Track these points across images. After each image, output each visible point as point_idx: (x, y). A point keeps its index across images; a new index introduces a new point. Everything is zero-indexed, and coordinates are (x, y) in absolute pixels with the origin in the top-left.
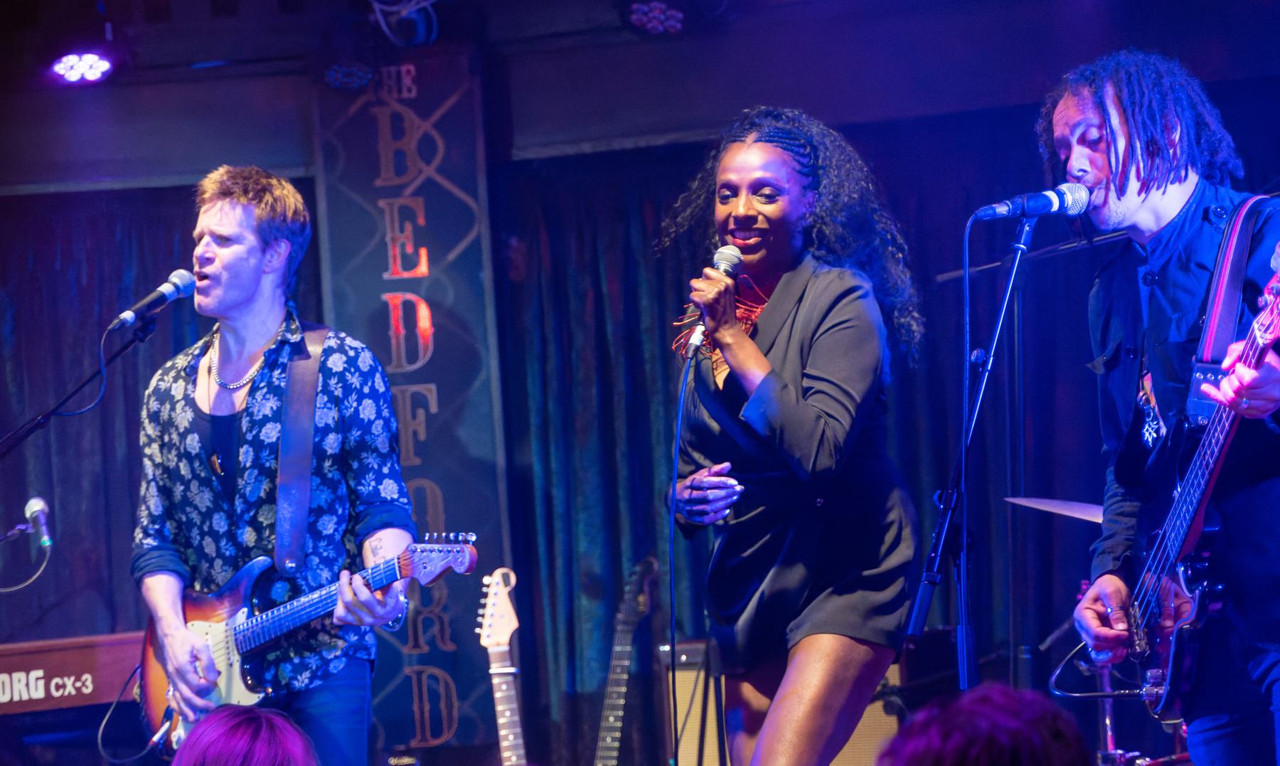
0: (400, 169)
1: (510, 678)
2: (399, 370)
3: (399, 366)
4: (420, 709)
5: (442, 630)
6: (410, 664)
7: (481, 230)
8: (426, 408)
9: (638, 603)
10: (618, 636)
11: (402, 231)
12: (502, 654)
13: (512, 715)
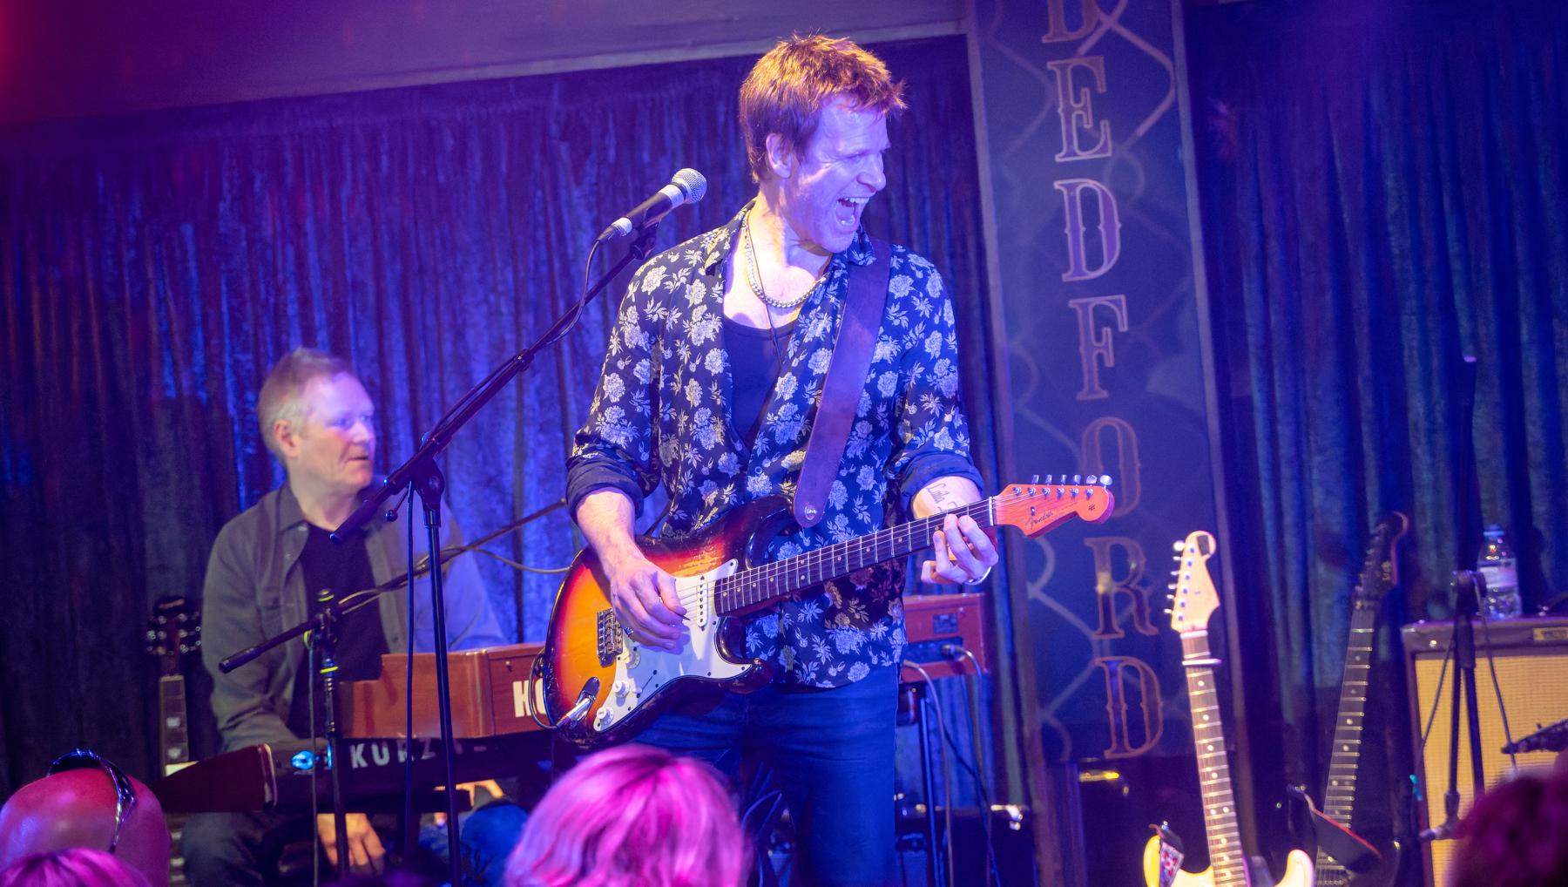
0: (1074, 24)
2: (1078, 278)
3: (1079, 272)
4: (1116, 711)
5: (1140, 610)
6: (1102, 655)
7: (1179, 94)
8: (1114, 326)
9: (1381, 570)
10: (1357, 616)
11: (1077, 100)
12: (1200, 639)
13: (1210, 721)
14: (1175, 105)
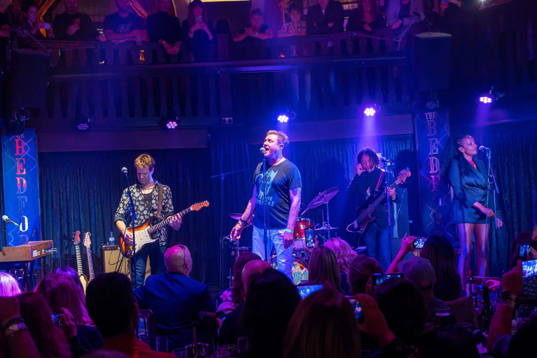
0: (20, 152)
1: (90, 253)
3: (19, 192)
7: (37, 165)
8: (25, 202)
14: (36, 167)
